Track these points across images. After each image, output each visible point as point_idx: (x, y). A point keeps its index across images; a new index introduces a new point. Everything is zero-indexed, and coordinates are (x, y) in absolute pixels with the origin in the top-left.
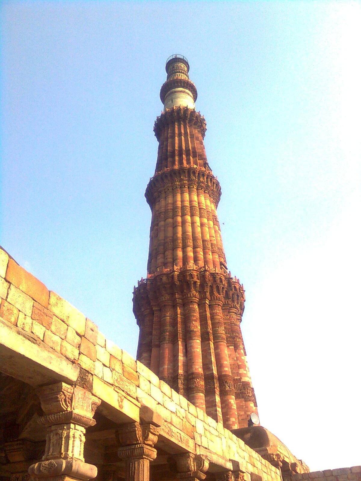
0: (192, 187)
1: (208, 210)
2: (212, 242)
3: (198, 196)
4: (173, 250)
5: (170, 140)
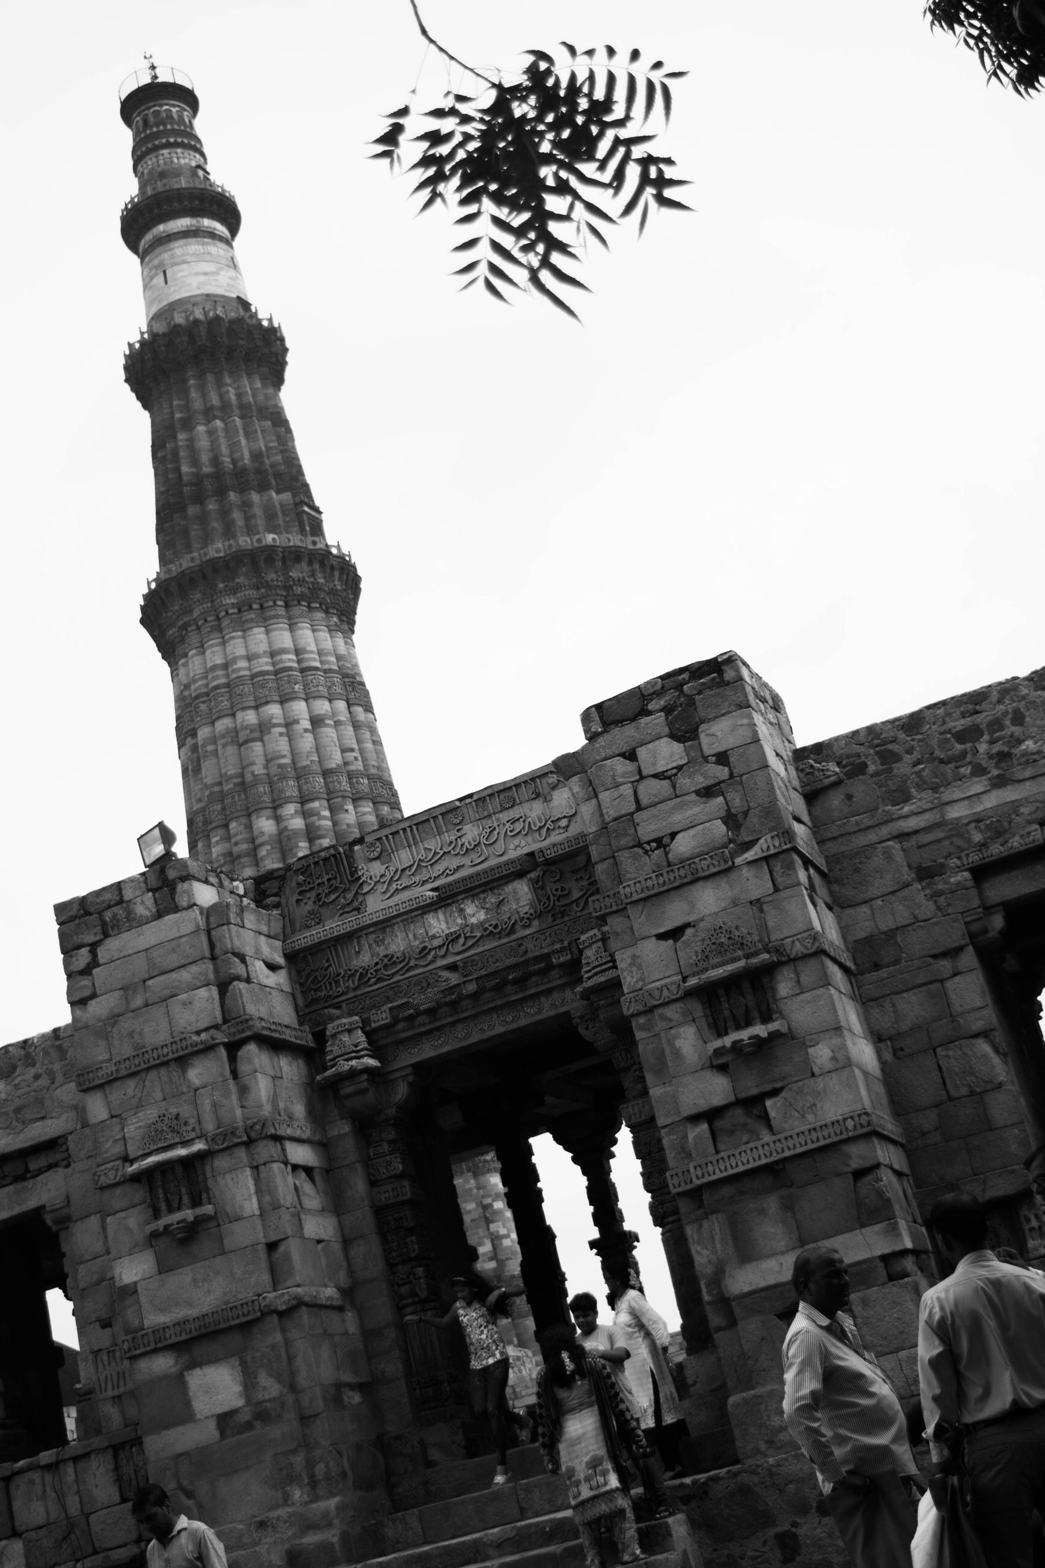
0: (271, 603)
1: (326, 667)
2: (352, 768)
3: (292, 627)
4: (249, 815)
5: (181, 436)
